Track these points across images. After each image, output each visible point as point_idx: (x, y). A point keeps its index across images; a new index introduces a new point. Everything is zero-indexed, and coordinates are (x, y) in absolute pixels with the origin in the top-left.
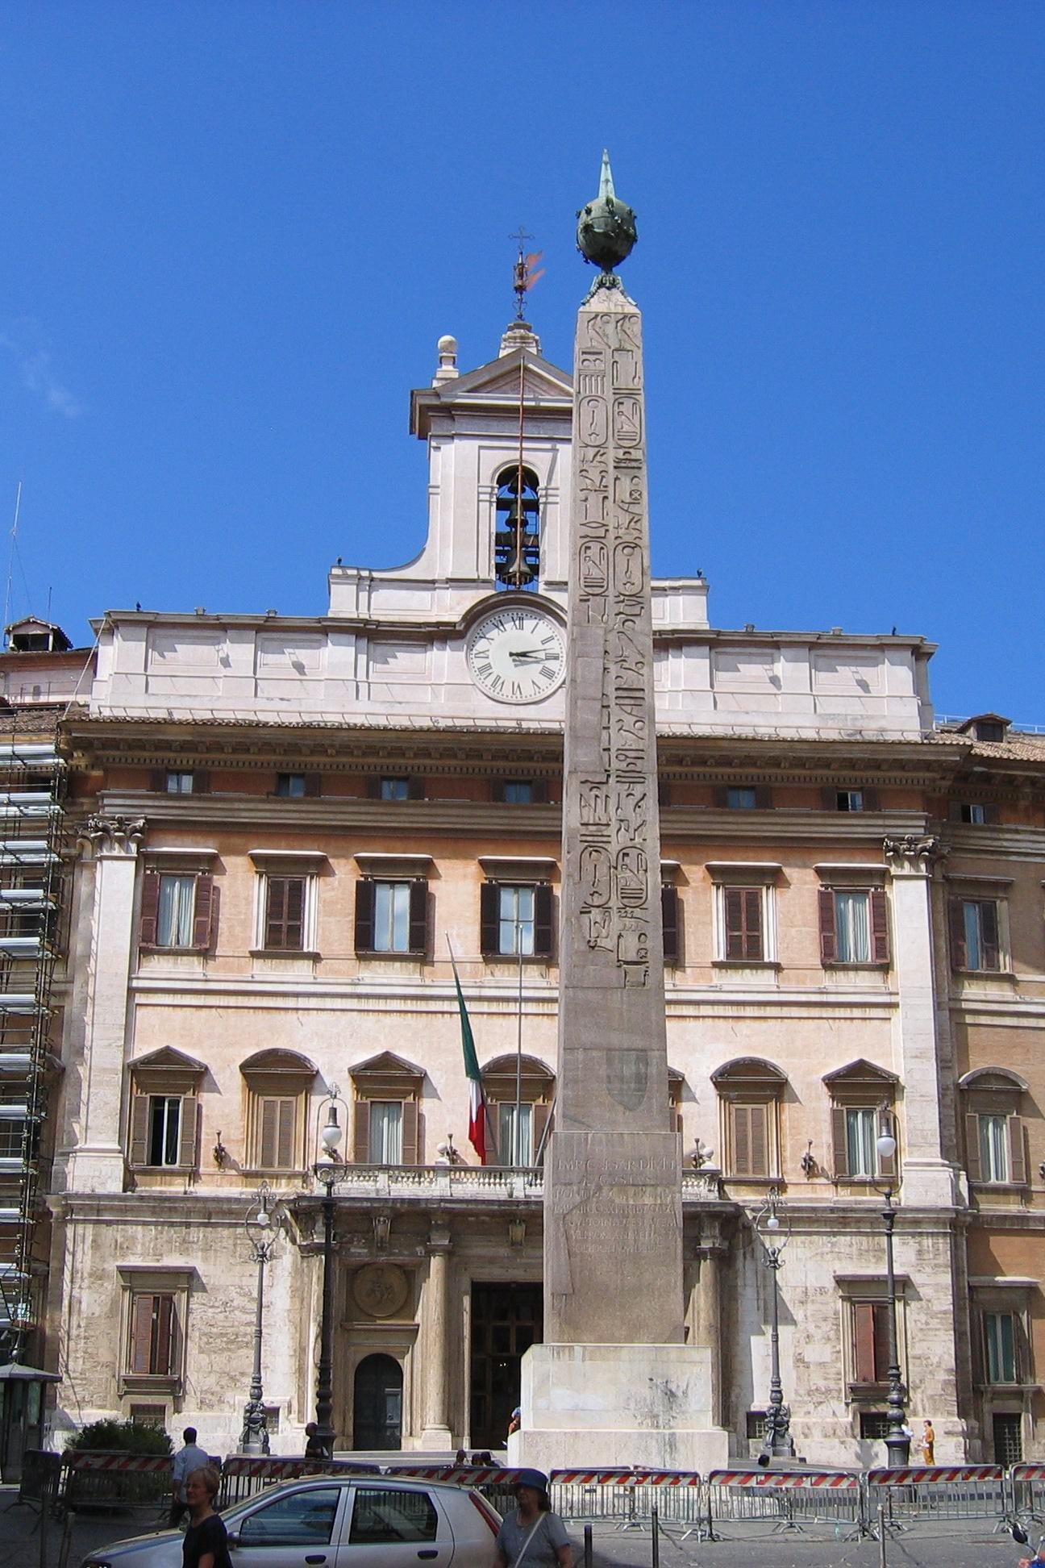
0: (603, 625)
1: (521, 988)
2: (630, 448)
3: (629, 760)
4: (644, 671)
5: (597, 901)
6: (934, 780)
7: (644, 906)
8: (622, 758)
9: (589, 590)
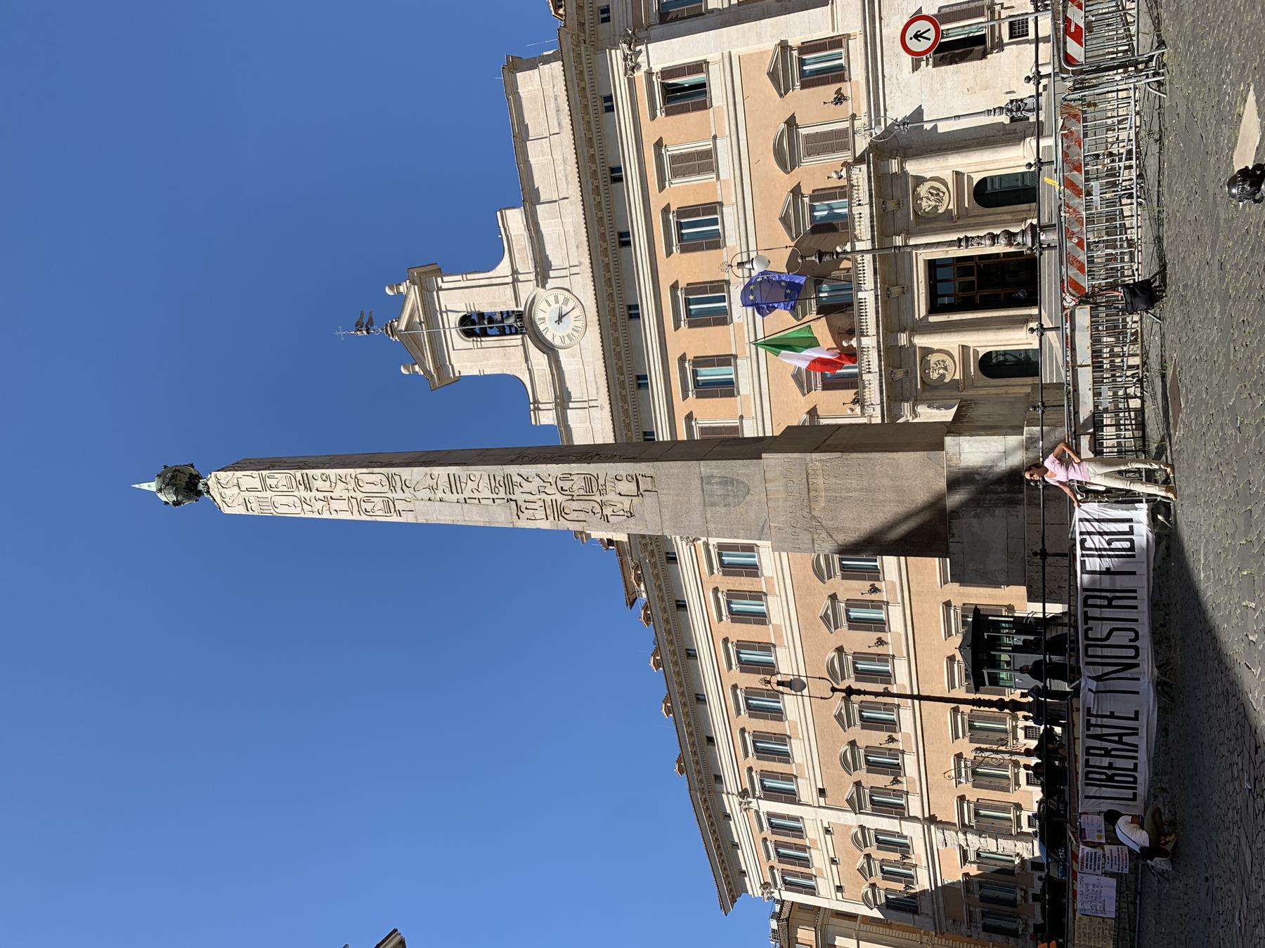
3: (498, 485)
5: (598, 509)
6: (586, 48)
9: (392, 510)
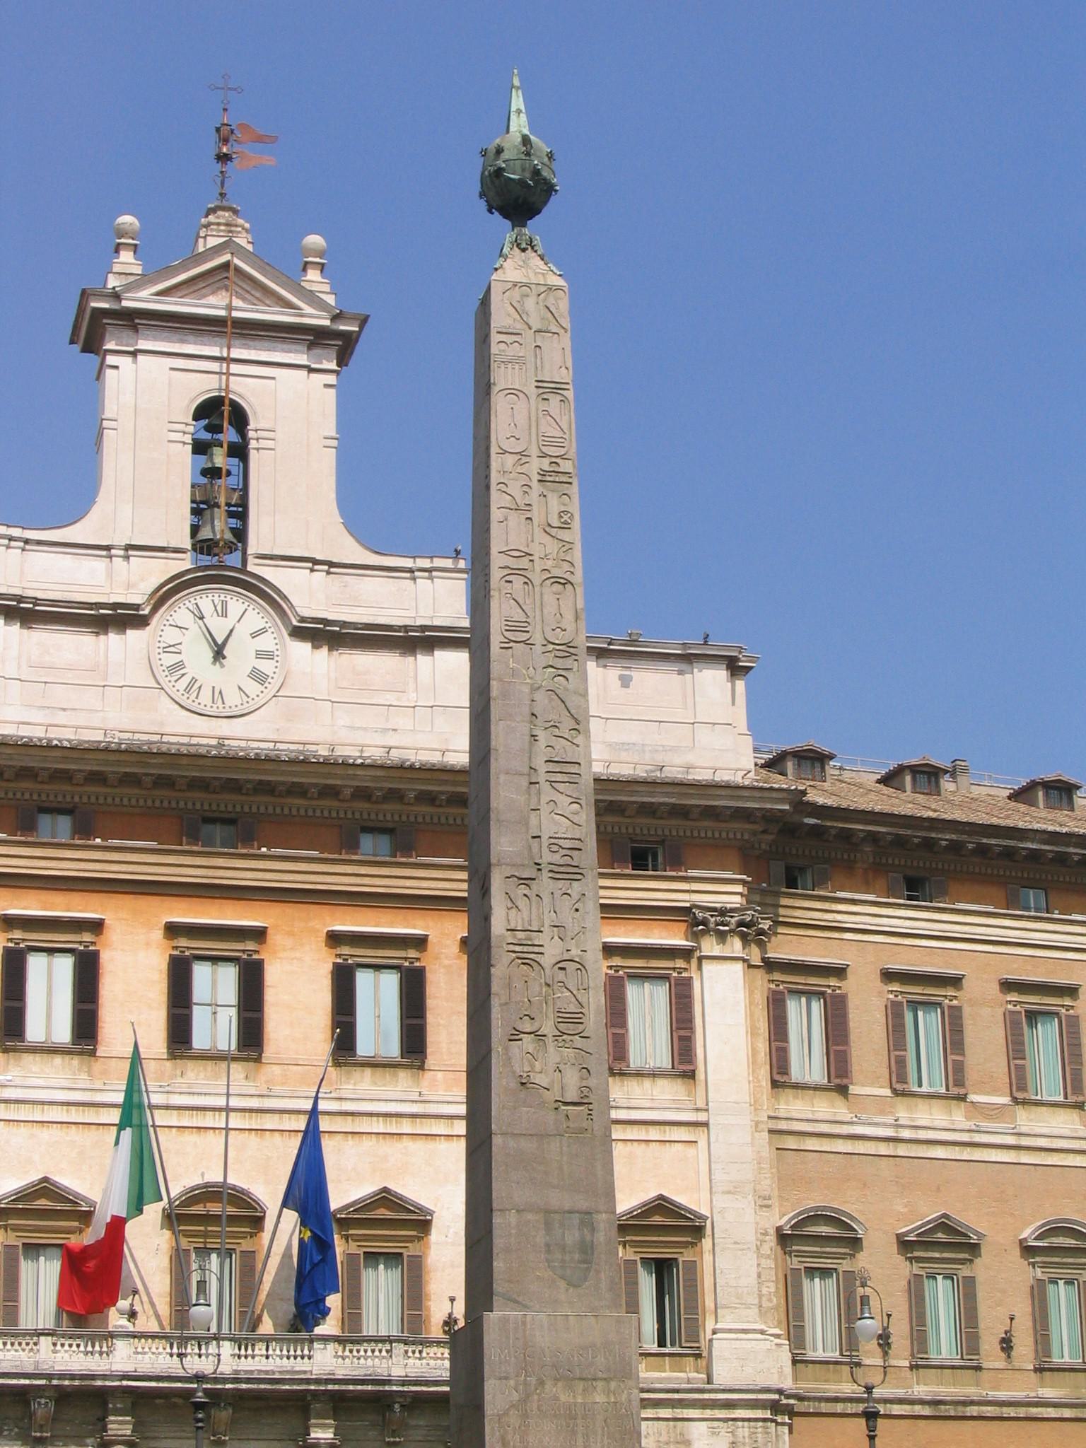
0: (528, 681)
1: (228, 1095)
2: (557, 457)
3: (565, 852)
4: (579, 740)
8: (555, 848)
9: (509, 635)
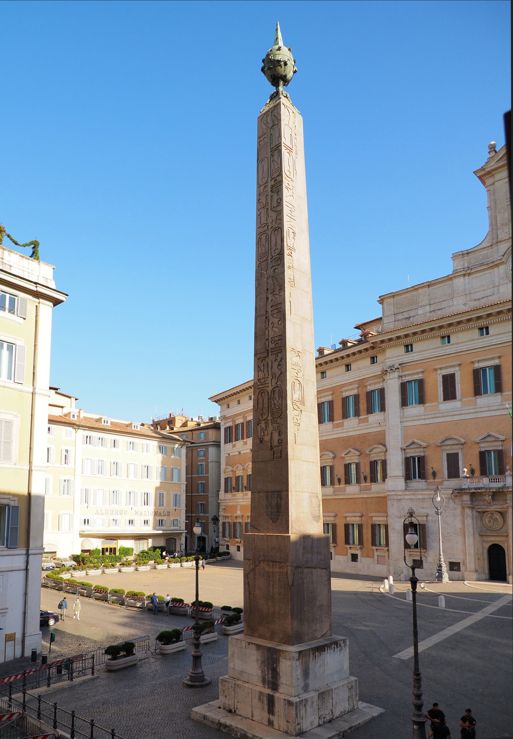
7: (281, 417)
